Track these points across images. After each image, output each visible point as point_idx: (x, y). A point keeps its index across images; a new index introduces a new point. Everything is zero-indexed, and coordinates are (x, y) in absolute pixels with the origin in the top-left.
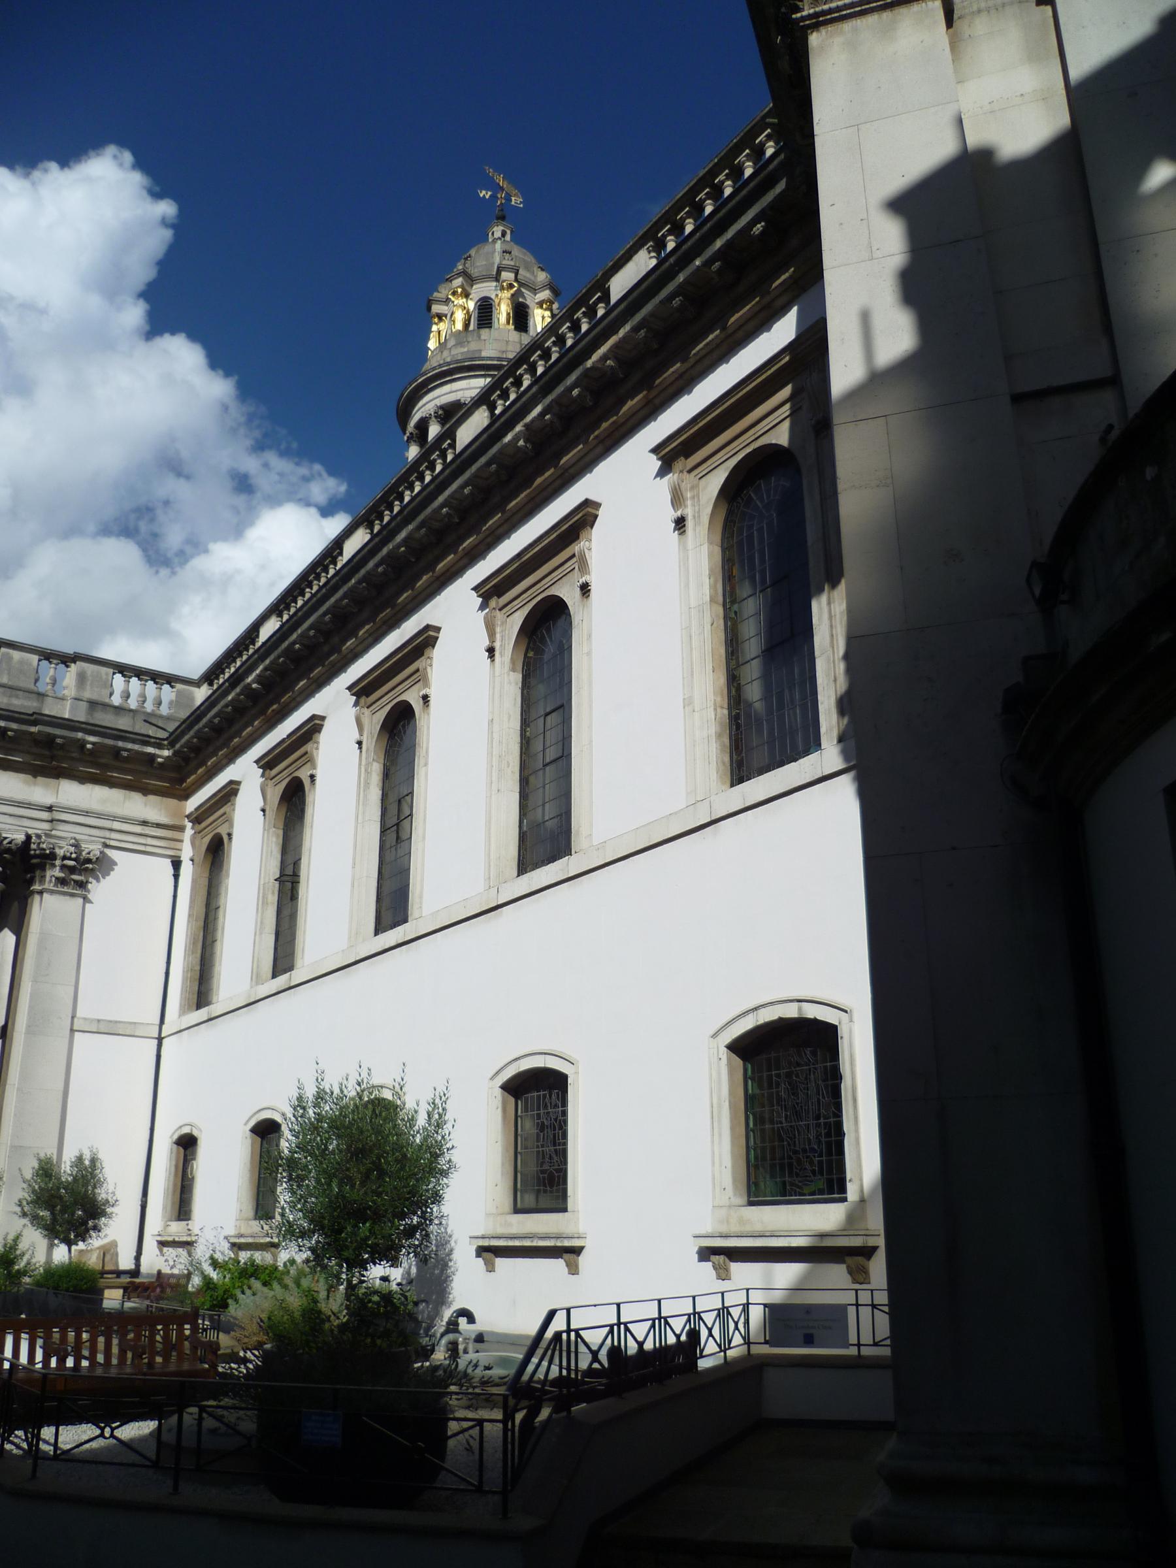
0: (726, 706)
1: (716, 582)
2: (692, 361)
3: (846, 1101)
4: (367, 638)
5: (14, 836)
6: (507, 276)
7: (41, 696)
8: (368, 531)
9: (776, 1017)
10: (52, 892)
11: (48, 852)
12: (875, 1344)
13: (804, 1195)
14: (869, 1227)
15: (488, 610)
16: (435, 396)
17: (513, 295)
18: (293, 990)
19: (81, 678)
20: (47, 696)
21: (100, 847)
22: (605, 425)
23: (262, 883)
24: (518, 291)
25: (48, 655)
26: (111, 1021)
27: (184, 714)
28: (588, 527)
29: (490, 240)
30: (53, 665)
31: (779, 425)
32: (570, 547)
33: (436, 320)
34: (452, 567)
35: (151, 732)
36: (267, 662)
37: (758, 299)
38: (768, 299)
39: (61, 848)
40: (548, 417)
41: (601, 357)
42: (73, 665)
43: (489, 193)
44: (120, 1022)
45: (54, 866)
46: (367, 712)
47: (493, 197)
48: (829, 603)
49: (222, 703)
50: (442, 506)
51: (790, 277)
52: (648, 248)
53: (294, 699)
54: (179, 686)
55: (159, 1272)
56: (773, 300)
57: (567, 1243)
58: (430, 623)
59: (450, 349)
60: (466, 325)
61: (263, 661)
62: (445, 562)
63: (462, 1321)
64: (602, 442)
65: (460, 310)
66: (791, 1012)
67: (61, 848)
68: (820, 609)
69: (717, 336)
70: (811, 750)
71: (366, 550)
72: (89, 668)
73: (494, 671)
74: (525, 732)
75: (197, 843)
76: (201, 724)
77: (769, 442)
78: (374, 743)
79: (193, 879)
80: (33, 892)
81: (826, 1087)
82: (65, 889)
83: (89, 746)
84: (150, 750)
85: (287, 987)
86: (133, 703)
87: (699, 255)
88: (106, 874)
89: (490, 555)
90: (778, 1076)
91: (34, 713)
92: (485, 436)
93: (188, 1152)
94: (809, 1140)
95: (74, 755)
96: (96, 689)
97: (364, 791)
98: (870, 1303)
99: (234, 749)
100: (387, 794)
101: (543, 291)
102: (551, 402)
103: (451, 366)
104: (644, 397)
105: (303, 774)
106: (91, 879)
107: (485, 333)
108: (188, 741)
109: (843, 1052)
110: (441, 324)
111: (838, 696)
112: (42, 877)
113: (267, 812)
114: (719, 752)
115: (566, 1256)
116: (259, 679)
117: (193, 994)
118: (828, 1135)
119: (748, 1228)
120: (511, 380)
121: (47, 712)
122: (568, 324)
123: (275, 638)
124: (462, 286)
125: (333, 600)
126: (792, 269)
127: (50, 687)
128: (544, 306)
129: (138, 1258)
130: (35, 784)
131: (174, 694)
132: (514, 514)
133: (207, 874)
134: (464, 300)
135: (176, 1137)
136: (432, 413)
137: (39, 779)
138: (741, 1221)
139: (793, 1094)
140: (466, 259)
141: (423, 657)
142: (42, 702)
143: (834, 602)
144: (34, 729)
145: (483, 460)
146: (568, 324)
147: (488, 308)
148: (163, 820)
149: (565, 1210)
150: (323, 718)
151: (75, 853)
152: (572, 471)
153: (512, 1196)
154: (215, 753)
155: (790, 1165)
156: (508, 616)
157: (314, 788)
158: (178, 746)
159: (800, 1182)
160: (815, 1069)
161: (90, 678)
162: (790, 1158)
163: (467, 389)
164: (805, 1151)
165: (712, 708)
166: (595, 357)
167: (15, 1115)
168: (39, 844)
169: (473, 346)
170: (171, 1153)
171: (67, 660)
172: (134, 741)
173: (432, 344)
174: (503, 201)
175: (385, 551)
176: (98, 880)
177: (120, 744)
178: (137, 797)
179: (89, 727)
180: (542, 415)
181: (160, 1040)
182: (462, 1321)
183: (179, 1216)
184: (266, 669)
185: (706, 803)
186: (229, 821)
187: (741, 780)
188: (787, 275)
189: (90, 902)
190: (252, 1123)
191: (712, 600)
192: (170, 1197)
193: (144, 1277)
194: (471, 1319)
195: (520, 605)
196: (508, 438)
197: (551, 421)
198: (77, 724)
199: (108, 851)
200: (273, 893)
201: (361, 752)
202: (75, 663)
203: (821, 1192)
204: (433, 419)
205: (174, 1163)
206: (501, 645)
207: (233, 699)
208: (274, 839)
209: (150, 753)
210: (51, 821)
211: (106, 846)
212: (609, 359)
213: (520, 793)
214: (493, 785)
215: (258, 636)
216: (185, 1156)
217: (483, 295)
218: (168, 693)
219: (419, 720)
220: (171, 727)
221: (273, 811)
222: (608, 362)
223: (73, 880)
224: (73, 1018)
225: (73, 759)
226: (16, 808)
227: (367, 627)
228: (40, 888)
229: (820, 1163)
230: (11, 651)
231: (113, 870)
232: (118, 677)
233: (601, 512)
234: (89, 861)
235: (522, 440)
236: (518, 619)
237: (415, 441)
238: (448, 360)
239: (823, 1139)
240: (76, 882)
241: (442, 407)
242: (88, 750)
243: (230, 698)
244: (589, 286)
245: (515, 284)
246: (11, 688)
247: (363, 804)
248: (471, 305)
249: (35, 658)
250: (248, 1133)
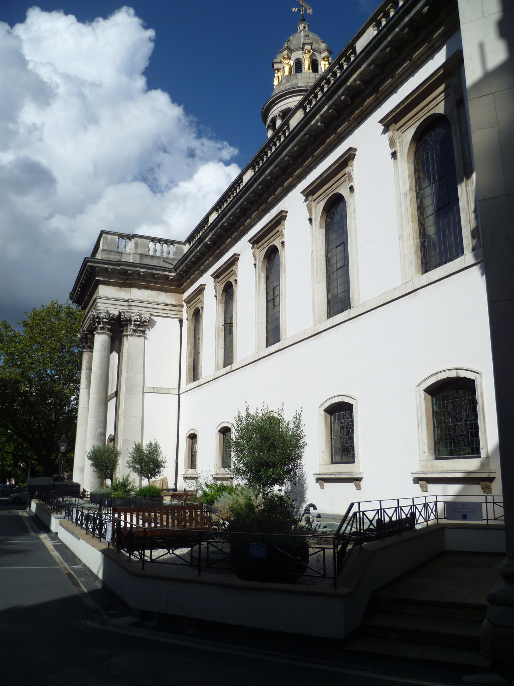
0: (418, 237)
1: (412, 180)
2: (396, 77)
3: (479, 413)
4: (256, 218)
6: (308, 47)
7: (121, 253)
8: (253, 170)
9: (446, 377)
10: (131, 335)
11: (128, 319)
12: (495, 519)
13: (461, 455)
14: (491, 469)
15: (308, 202)
16: (278, 107)
17: (310, 56)
18: (233, 372)
19: (136, 244)
20: (123, 253)
21: (149, 316)
22: (357, 112)
23: (217, 327)
24: (313, 53)
25: (122, 236)
26: (159, 388)
27: (180, 257)
28: (352, 160)
29: (299, 31)
30: (124, 240)
31: (440, 104)
32: (344, 170)
33: (276, 71)
34: (291, 183)
35: (167, 265)
36: (213, 232)
37: (427, 44)
38: (431, 43)
39: (133, 317)
40: (330, 111)
41: (353, 80)
42: (132, 239)
43: (297, 9)
44: (162, 388)
45: (131, 324)
46: (257, 251)
47: (299, 11)
48: (466, 187)
49: (195, 251)
50: (285, 156)
51: (442, 31)
52: (373, 26)
53: (226, 247)
54: (177, 245)
55: (185, 489)
56: (434, 44)
57: (355, 476)
58: (283, 210)
59: (284, 84)
60: (290, 72)
61: (211, 232)
62: (288, 181)
63: (311, 509)
64: (356, 120)
65: (287, 66)
66: (453, 374)
67: (133, 317)
68: (462, 189)
69: (408, 64)
70: (459, 256)
71: (253, 179)
72: (139, 240)
73: (312, 230)
74: (328, 256)
75: (189, 311)
76: (187, 261)
77: (435, 112)
78: (261, 266)
79: (188, 327)
80: (123, 336)
81: (470, 407)
82: (136, 334)
83: (141, 273)
84: (167, 273)
85: (230, 371)
86: (158, 254)
87: (397, 26)
88: (153, 327)
90: (448, 403)
91: (118, 261)
92: (302, 122)
93: (193, 441)
94: (462, 430)
95: (135, 277)
96: (142, 249)
97: (258, 285)
98: (492, 502)
99: (202, 271)
100: (268, 286)
101: (324, 52)
102: (332, 104)
103: (285, 92)
104: (375, 97)
105: (232, 280)
106: (146, 329)
107: (299, 75)
108: (182, 269)
109: (478, 391)
110: (279, 73)
111: (472, 229)
112: (127, 329)
113: (217, 297)
114: (416, 259)
115: (355, 482)
116: (210, 239)
117: (191, 376)
118: (471, 428)
119: (435, 470)
120: (313, 95)
121: (123, 260)
122: (337, 66)
123: (216, 221)
124: (287, 55)
125: (240, 202)
126: (443, 27)
127: (124, 249)
128: (325, 59)
129: (176, 484)
130: (121, 291)
131: (175, 249)
132: (317, 157)
133: (193, 325)
134: (289, 61)
135: (188, 435)
137: (122, 288)
138: (432, 466)
139: (455, 411)
140: (288, 41)
141: (280, 225)
142: (121, 256)
143: (468, 186)
144: (119, 268)
145: (302, 134)
146: (337, 66)
147: (299, 63)
148: (174, 303)
149: (354, 462)
150: (239, 255)
151: (139, 319)
152: (342, 135)
153: (330, 458)
154: (194, 273)
155: (454, 442)
156: (317, 204)
157: (237, 286)
158: (178, 271)
159: (458, 449)
160: (465, 399)
161: (140, 244)
162: (454, 439)
163: (292, 102)
164: (460, 436)
165: (412, 239)
166: (351, 80)
167: (123, 427)
168: (124, 316)
169: (294, 82)
170: (187, 441)
171: (130, 237)
172: (160, 270)
173: (275, 83)
174: (303, 12)
175: (261, 179)
176: (149, 330)
177: (154, 271)
178: (163, 294)
179: (141, 265)
180: (328, 110)
181: (179, 395)
182: (311, 509)
183: (191, 467)
184: (213, 235)
185: (411, 283)
186: (202, 302)
187: (427, 271)
188: (440, 31)
189: (147, 339)
190: (219, 428)
191: (411, 189)
192: (187, 459)
193: (179, 492)
194: (315, 508)
195: (322, 198)
197: (332, 113)
198: (136, 264)
199: (152, 317)
200: (222, 331)
201: (256, 268)
202: (133, 238)
203: (469, 454)
204: (278, 117)
205: (188, 445)
206: (315, 217)
207: (200, 249)
208: (221, 308)
209: (167, 275)
210: (129, 306)
211: (152, 315)
212: (358, 80)
213: (327, 282)
214: (315, 279)
215: (208, 221)
216: (192, 442)
217: (297, 57)
218: (172, 248)
219: (280, 252)
220: (175, 263)
221: (220, 296)
222: (357, 82)
223: (139, 330)
224: (143, 387)
225: (135, 279)
226: (114, 301)
227: (255, 213)
228: (126, 334)
229: (468, 441)
230: (107, 235)
231: (155, 325)
232: (151, 243)
233: (357, 153)
234: (145, 322)
235: (319, 123)
236: (322, 204)
237: (270, 128)
238: (283, 89)
239: (469, 431)
240: (141, 331)
241: (281, 112)
242: (141, 275)
243: (198, 249)
244: (346, 47)
245: (311, 51)
246: (108, 251)
247: (258, 291)
248: (292, 63)
249: (117, 237)
250: (218, 433)
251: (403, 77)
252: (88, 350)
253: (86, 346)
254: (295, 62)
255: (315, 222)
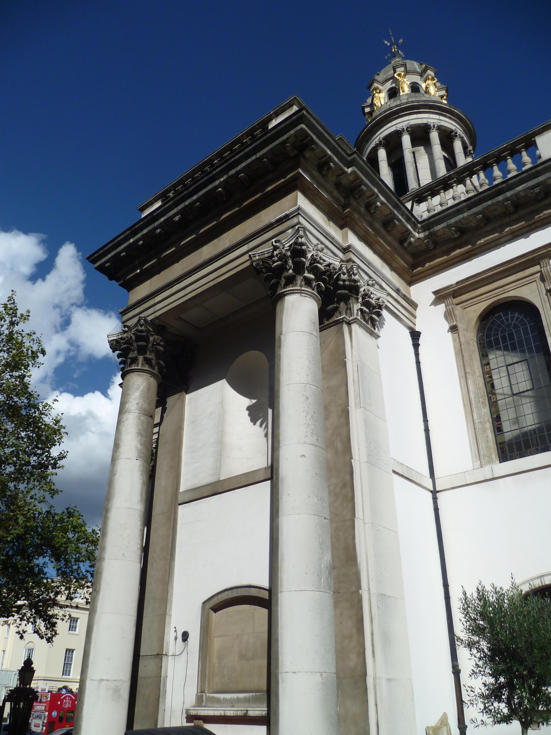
5: (331, 261)
103: (420, 103)
136: (405, 129)
181: (434, 493)
252: (147, 368)
253: (141, 358)
254: (411, 85)
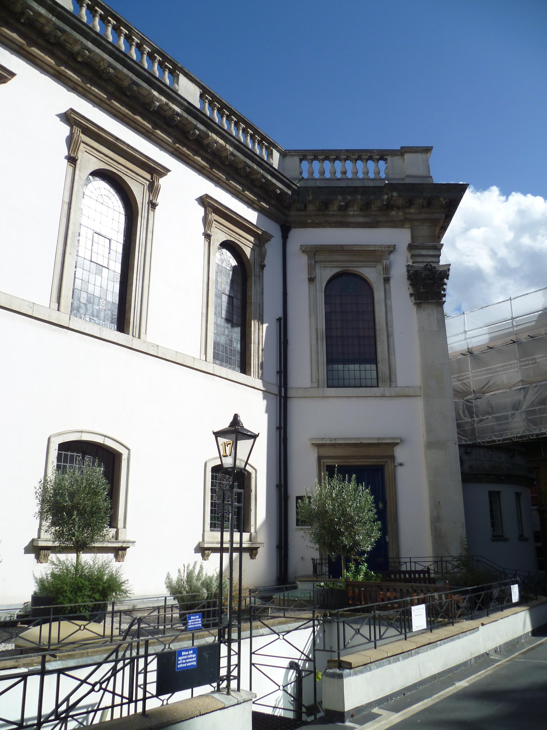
22: (185, 149)
89: (73, 94)
104: (206, 167)
152: (153, 137)
156: (86, 151)
166: (214, 136)
180: (178, 114)
196: (155, 93)
251: (227, 187)
255: (80, 171)
